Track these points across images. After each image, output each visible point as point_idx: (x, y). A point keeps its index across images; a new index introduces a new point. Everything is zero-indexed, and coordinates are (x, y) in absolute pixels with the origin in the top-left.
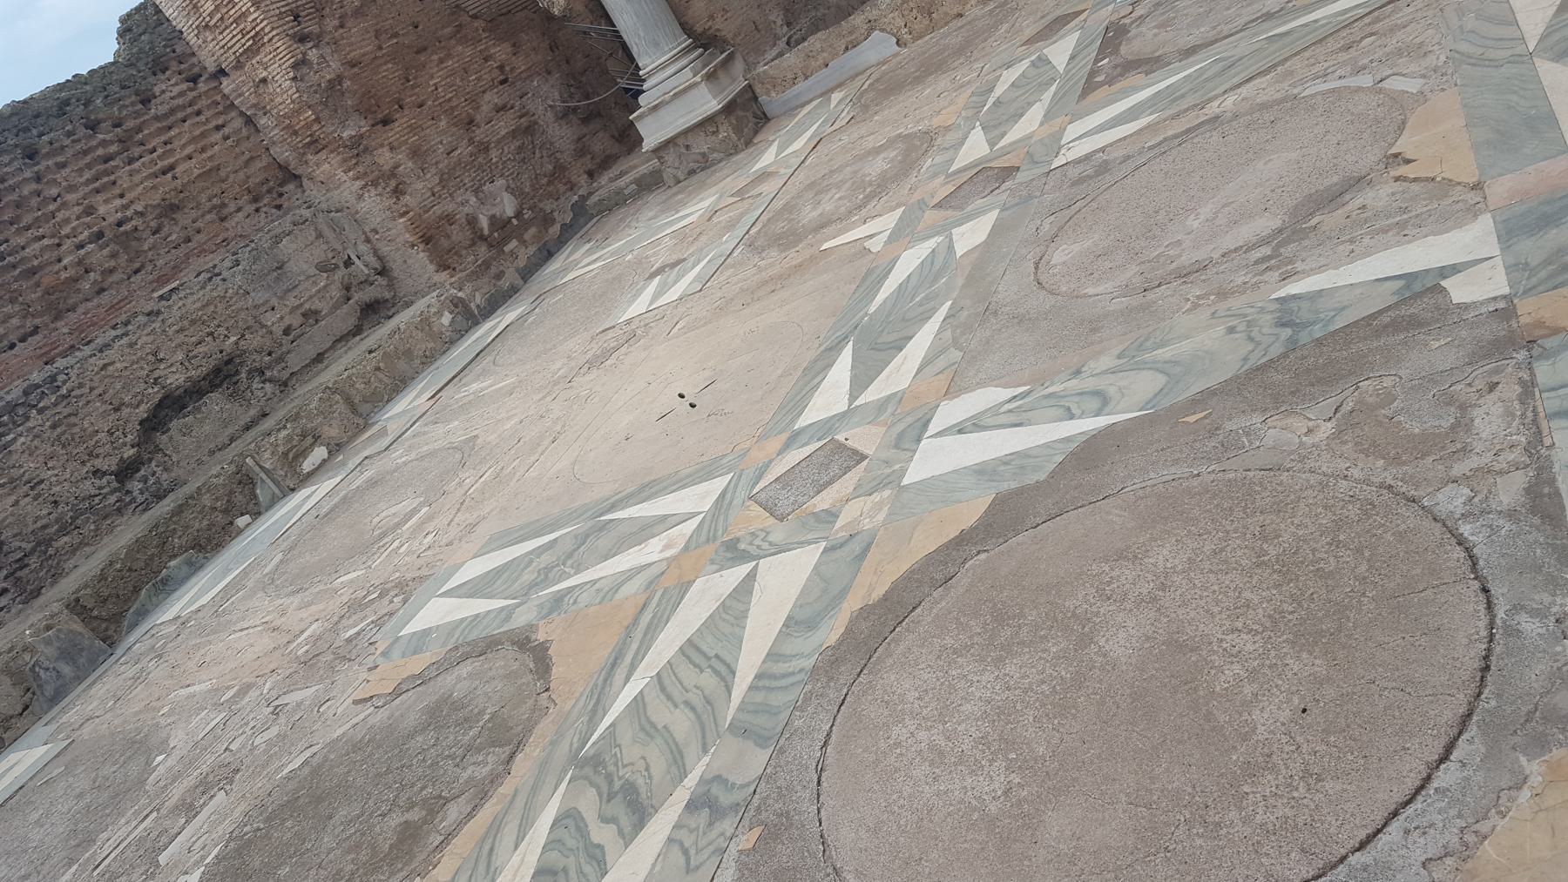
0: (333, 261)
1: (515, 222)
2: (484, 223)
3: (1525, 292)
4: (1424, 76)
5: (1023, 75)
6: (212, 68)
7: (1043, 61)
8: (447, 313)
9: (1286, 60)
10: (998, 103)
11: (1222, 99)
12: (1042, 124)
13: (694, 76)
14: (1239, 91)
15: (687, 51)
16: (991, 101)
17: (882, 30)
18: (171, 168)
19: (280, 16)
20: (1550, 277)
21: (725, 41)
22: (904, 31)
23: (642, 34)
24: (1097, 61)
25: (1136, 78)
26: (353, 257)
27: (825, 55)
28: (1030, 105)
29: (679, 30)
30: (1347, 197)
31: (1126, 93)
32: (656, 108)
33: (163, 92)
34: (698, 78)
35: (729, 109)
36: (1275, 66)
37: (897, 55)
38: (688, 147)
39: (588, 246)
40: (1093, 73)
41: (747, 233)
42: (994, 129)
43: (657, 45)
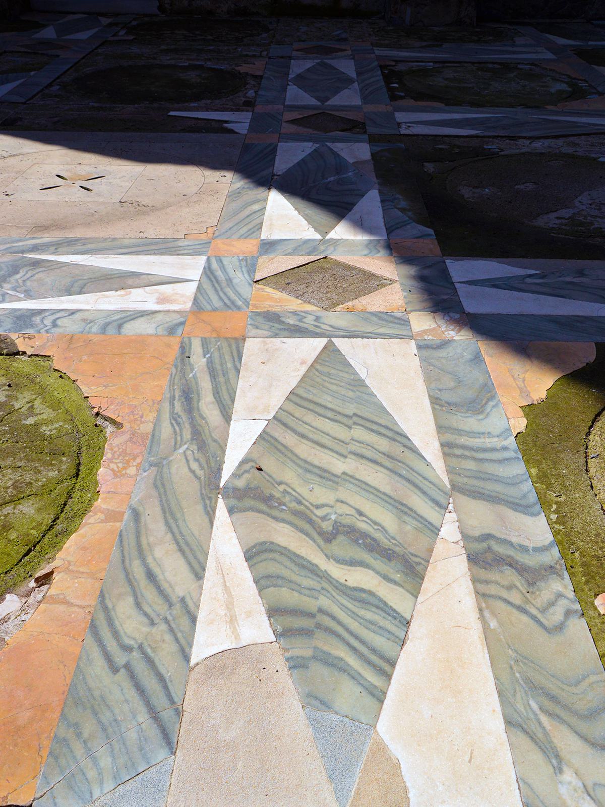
41: (58, 78)
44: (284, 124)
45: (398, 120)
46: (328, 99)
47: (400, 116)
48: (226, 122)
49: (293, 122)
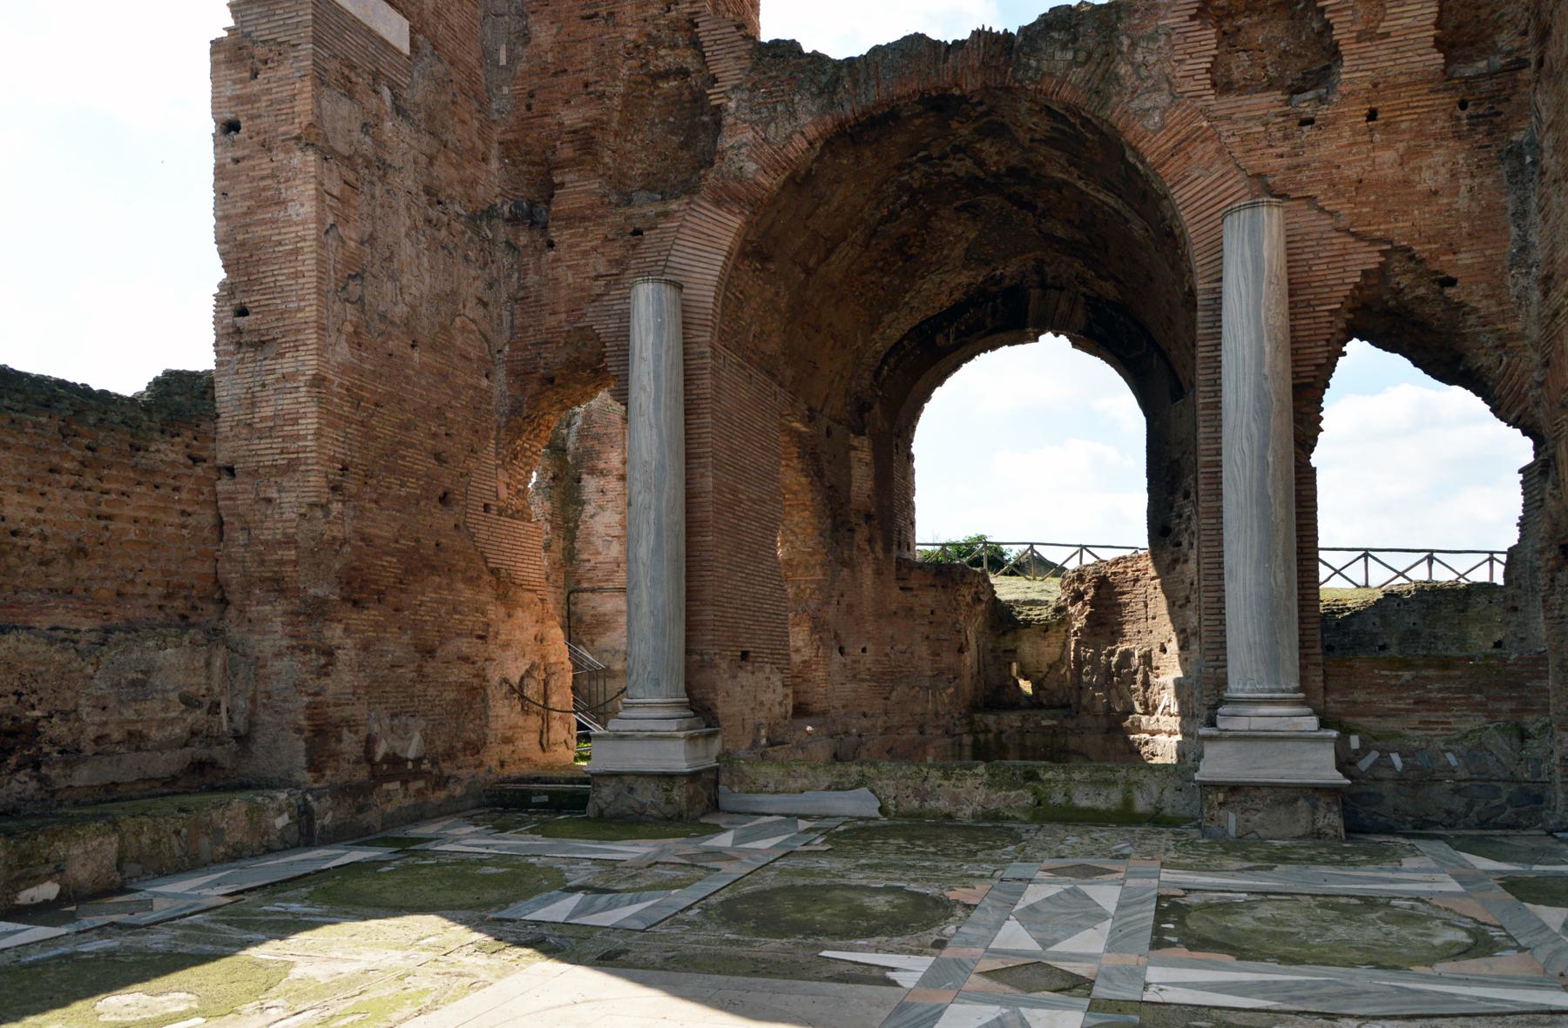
0: (200, 699)
1: (410, 765)
2: (381, 750)
6: (221, 462)
8: (286, 816)
15: (679, 705)
17: (873, 791)
18: (109, 518)
19: (332, 459)
21: (715, 718)
22: (891, 801)
23: (649, 668)
26: (223, 707)
27: (806, 781)
29: (682, 685)
32: (622, 737)
33: (158, 451)
34: (681, 734)
35: (693, 776)
37: (876, 819)
38: (631, 790)
39: (473, 829)
41: (704, 898)
43: (657, 683)
44: (973, 977)
45: (1148, 979)
46: (1055, 942)
47: (1154, 974)
48: (893, 969)
49: (986, 974)
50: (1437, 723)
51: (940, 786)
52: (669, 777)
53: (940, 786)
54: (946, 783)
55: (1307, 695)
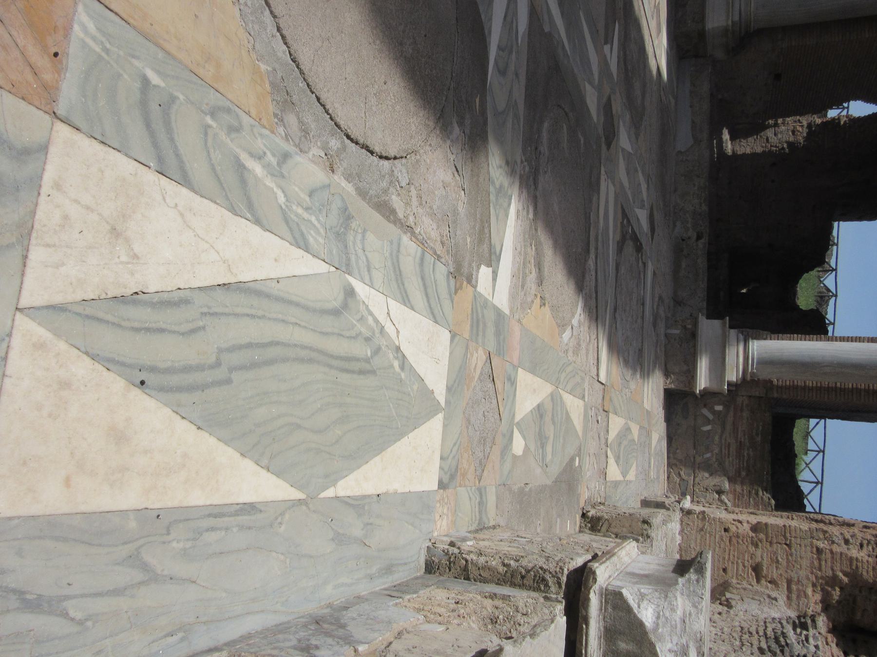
3: (475, 296)
4: (567, 344)
5: (641, 192)
7: (642, 207)
9: (597, 299)
10: (636, 171)
11: (594, 261)
12: (620, 179)
13: (732, 22)
14: (594, 271)
16: (639, 169)
20: (477, 312)
24: (632, 228)
25: (618, 237)
28: (630, 183)
30: (537, 270)
31: (615, 226)
34: (730, 23)
35: (702, 34)
36: (596, 292)
40: (629, 221)
42: (628, 157)
50: (729, 451)
51: (694, 185)
52: (702, 19)
53: (694, 185)
54: (696, 188)
55: (747, 382)
